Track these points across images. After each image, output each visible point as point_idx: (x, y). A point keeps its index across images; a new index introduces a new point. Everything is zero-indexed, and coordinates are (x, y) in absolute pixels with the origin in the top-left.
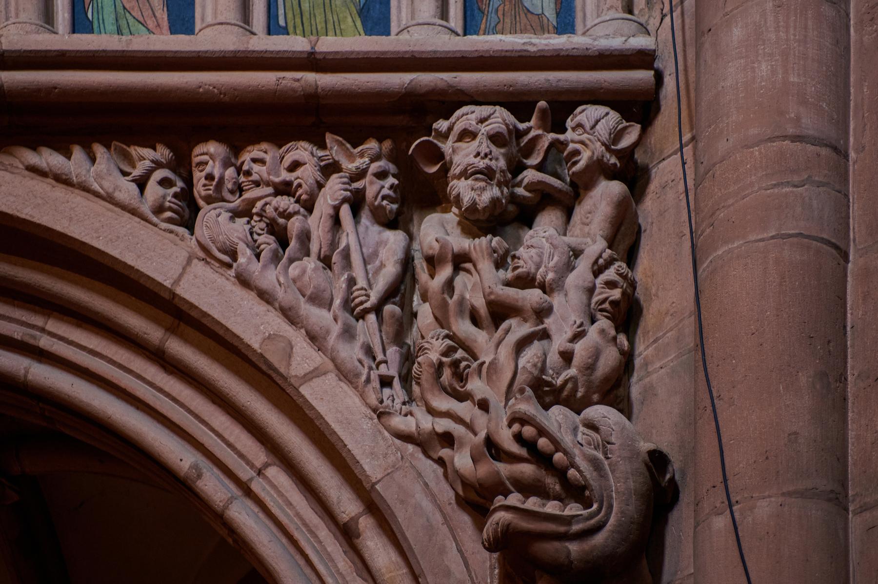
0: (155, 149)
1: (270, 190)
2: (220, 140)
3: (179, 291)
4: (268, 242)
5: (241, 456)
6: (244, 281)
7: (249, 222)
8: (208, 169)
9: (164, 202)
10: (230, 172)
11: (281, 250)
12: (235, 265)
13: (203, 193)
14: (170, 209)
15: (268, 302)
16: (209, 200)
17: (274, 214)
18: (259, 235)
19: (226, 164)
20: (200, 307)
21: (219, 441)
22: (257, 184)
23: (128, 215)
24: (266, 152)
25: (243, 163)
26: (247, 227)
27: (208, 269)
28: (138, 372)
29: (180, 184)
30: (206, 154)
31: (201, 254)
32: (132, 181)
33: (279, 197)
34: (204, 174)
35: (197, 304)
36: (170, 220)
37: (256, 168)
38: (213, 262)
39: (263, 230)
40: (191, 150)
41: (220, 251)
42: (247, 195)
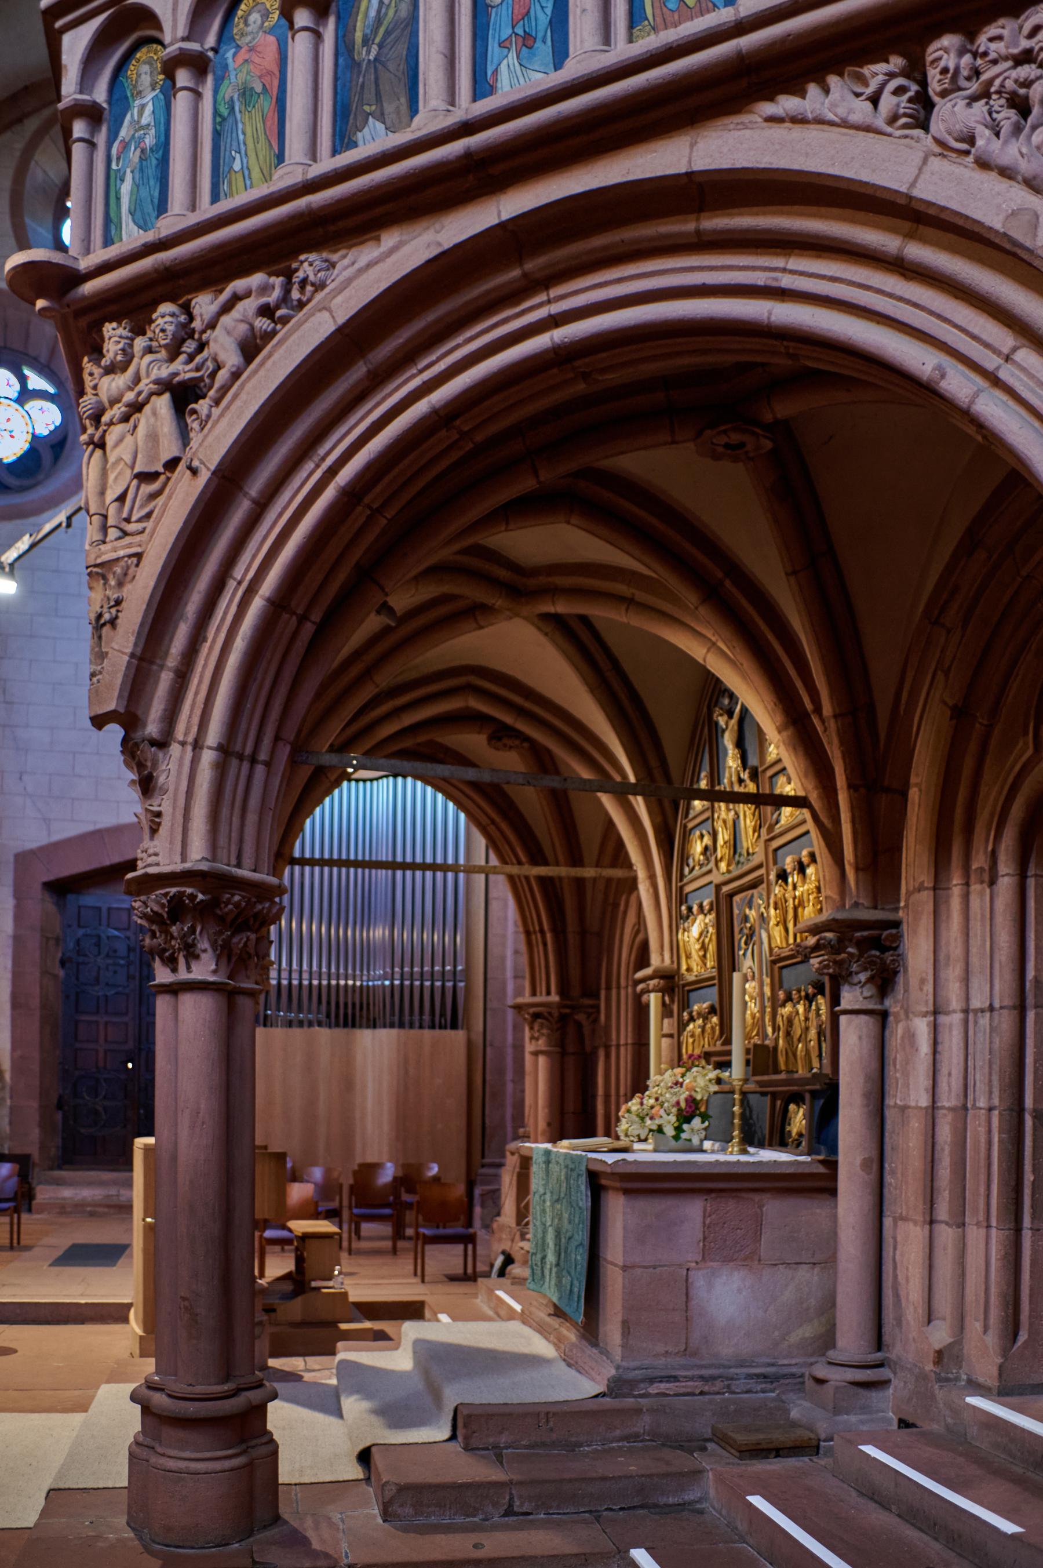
0: (887, 61)
1: (1010, 63)
2: (953, 30)
3: (916, 193)
4: (1007, 117)
5: (987, 345)
6: (983, 164)
7: (987, 103)
8: (942, 64)
9: (897, 110)
10: (967, 58)
11: (1023, 122)
12: (973, 150)
13: (938, 89)
14: (905, 115)
15: (1010, 178)
16: (944, 94)
17: (1015, 87)
18: (998, 112)
19: (961, 53)
20: (939, 203)
21: (963, 336)
22: (995, 62)
23: (862, 134)
24: (1003, 27)
25: (979, 46)
26: (985, 109)
27: (945, 162)
28: (877, 286)
29: (914, 88)
30: (941, 49)
31: (938, 150)
32: (866, 99)
33: (1019, 69)
34: (938, 69)
35: (934, 201)
36: (905, 126)
37: (993, 46)
38: (950, 154)
39: (1002, 106)
40: (924, 51)
41: (957, 140)
42: (984, 77)
